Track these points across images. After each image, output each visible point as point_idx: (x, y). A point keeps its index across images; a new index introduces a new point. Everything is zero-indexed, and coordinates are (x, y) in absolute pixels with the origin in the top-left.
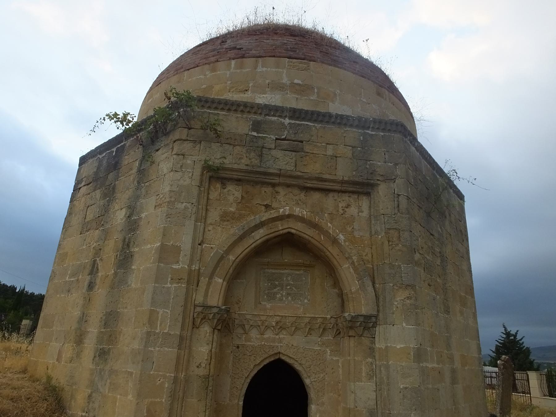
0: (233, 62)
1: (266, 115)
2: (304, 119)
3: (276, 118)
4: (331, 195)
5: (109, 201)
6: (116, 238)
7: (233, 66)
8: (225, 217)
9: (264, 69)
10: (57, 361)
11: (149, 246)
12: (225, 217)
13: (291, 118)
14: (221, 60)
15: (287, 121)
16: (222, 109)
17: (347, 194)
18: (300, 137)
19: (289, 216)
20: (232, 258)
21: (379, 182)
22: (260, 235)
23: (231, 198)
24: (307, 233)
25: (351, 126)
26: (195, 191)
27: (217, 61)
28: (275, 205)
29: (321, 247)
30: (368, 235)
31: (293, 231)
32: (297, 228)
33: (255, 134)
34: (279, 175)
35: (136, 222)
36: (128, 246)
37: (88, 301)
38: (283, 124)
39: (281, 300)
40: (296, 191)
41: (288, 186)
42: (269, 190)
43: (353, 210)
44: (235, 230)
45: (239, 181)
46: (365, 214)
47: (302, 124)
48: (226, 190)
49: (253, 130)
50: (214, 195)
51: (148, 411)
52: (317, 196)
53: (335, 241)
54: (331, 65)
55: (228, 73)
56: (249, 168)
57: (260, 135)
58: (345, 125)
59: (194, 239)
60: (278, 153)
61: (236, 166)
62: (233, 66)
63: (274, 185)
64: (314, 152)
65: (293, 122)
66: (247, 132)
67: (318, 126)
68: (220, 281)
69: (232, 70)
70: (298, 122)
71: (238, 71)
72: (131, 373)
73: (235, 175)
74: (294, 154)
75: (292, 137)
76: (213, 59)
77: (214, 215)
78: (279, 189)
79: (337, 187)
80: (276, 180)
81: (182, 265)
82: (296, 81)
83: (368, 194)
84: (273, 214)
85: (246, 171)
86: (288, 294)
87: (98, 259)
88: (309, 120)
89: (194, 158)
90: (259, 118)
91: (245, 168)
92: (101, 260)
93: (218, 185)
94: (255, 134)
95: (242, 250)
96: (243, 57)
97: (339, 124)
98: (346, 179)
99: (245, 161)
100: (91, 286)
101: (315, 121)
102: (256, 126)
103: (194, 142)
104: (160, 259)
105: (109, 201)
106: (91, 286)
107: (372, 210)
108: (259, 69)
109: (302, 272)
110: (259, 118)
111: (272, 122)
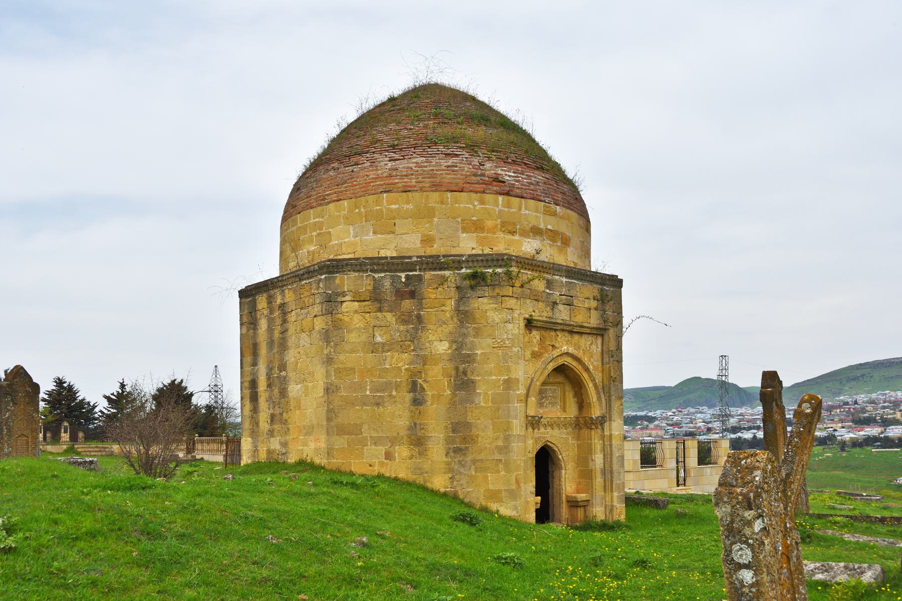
0: (500, 198)
1: (554, 275)
2: (573, 278)
3: (558, 277)
4: (583, 336)
5: (416, 329)
7: (500, 202)
9: (527, 212)
10: (386, 459)
11: (494, 378)
12: (535, 355)
13: (566, 277)
14: (488, 192)
15: (564, 280)
16: (529, 269)
17: (591, 335)
19: (567, 354)
21: (609, 328)
22: (551, 367)
23: (535, 341)
24: (573, 364)
25: (597, 283)
27: (484, 192)
28: (557, 345)
29: (579, 373)
30: (600, 364)
31: (566, 363)
32: (568, 361)
33: (548, 291)
34: (560, 324)
35: (469, 355)
36: (465, 373)
38: (562, 282)
39: (546, 407)
40: (567, 334)
41: (563, 330)
42: (553, 333)
43: (594, 347)
46: (599, 349)
47: (572, 282)
48: (531, 335)
51: (516, 479)
52: (576, 337)
53: (587, 369)
55: (497, 210)
56: (548, 320)
57: (551, 292)
58: (594, 282)
60: (561, 307)
61: (540, 318)
62: (500, 202)
63: (556, 330)
64: (579, 305)
65: (567, 280)
66: (543, 289)
67: (580, 283)
68: (534, 399)
69: (500, 206)
70: (570, 280)
71: (506, 209)
72: (500, 460)
74: (569, 307)
76: (479, 187)
78: (558, 333)
79: (588, 331)
80: (559, 327)
81: (522, 391)
82: (549, 227)
83: (602, 335)
84: (556, 353)
85: (546, 322)
86: (550, 403)
87: (420, 381)
88: (575, 279)
91: (545, 319)
92: (425, 381)
94: (548, 291)
95: (542, 379)
96: (508, 194)
97: (591, 281)
98: (595, 326)
99: (545, 314)
100: (417, 402)
101: (578, 279)
103: (517, 298)
105: (416, 329)
106: (417, 402)
107: (604, 347)
108: (524, 211)
109: (556, 387)
110: (549, 277)
111: (557, 281)
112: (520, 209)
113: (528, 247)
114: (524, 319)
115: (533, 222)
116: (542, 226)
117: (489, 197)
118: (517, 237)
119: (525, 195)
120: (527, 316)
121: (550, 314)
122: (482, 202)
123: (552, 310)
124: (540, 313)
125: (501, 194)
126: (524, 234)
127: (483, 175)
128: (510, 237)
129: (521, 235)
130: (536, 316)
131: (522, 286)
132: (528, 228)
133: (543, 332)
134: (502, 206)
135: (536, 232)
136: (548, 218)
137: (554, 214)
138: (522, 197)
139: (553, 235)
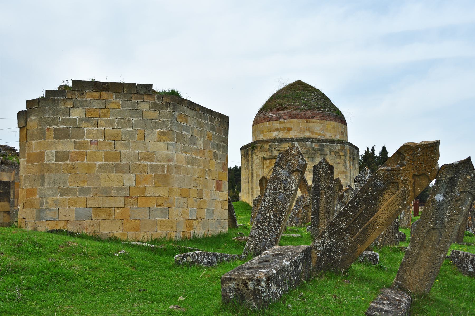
0: (268, 123)
6: (251, 172)
8: (267, 167)
12: (267, 167)
13: (277, 143)
15: (276, 143)
18: (279, 147)
20: (269, 175)
23: (268, 163)
26: (261, 163)
37: (249, 185)
38: (275, 144)
44: (269, 169)
45: (269, 159)
49: (270, 147)
50: (264, 163)
54: (290, 119)
59: (262, 172)
60: (275, 152)
67: (283, 143)
73: (268, 158)
75: (278, 147)
77: (265, 167)
82: (282, 127)
88: (281, 142)
89: (259, 156)
90: (271, 144)
93: (265, 160)
96: (269, 121)
99: (269, 155)
101: (282, 142)
102: (270, 146)
104: (257, 177)
108: (273, 125)
110: (271, 144)
111: (273, 144)
112: (272, 124)
113: (274, 134)
114: (262, 157)
115: (276, 127)
116: (279, 127)
117: (265, 123)
118: (272, 133)
119: (274, 120)
120: (262, 156)
121: (271, 155)
122: (264, 125)
123: (272, 153)
124: (266, 154)
125: (267, 121)
126: (274, 131)
127: (265, 117)
128: (270, 133)
129: (273, 132)
130: (265, 156)
131: (261, 148)
132: (274, 129)
133: (271, 160)
134: (268, 125)
135: (277, 130)
136: (281, 125)
137: (284, 123)
138: (273, 121)
139: (283, 129)
